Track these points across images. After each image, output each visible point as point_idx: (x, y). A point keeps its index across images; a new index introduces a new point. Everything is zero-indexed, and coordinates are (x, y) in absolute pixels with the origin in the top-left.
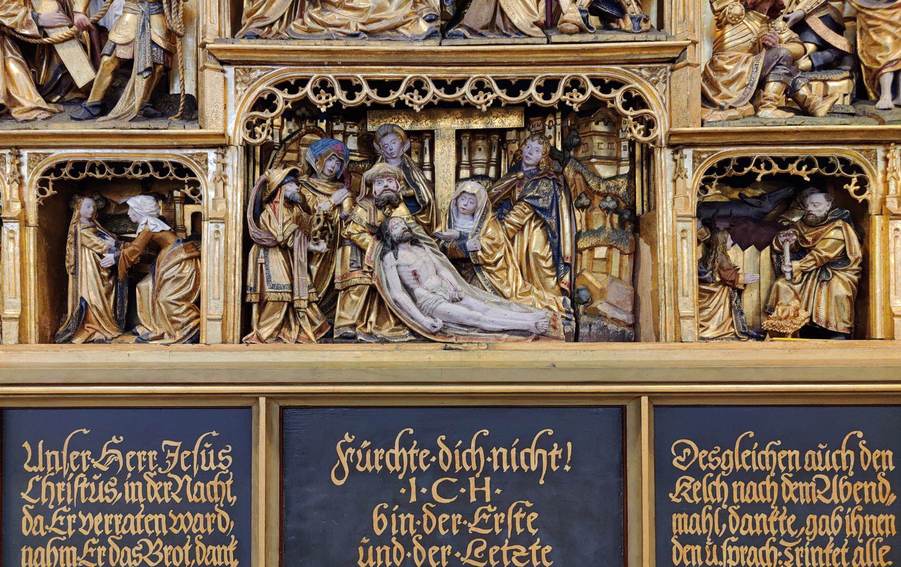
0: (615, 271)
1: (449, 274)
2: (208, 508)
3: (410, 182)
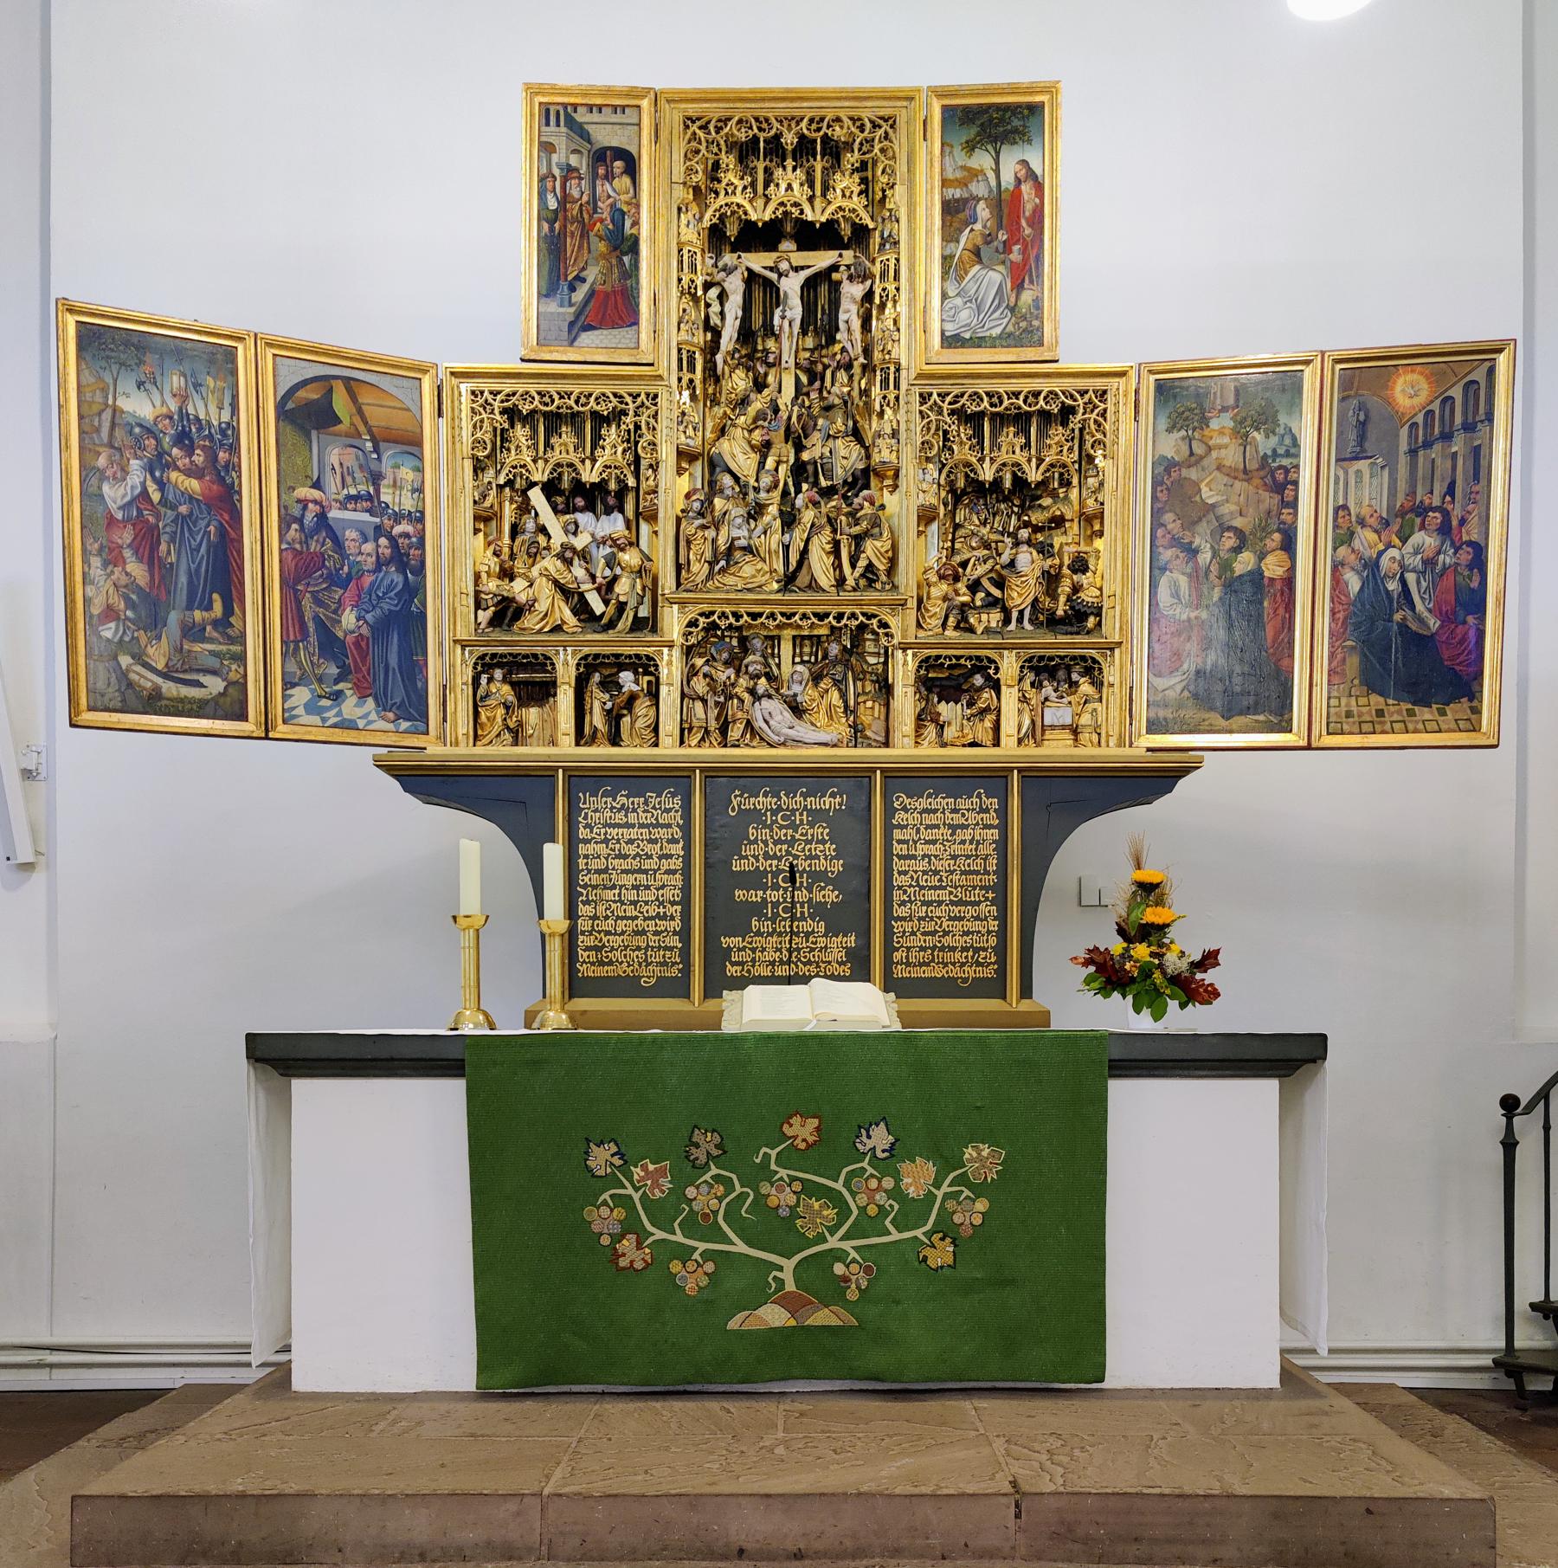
2: (669, 826)
3: (767, 665)
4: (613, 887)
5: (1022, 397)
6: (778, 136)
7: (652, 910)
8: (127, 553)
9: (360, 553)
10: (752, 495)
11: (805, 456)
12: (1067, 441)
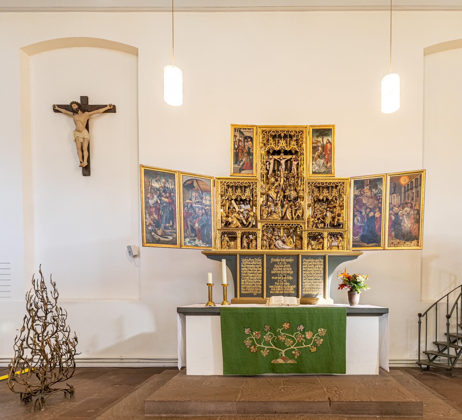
1: (282, 243)
2: (259, 265)
3: (278, 234)
4: (248, 276)
6: (280, 134)
7: (256, 281)
8: (154, 213)
10: (275, 202)
11: (286, 194)
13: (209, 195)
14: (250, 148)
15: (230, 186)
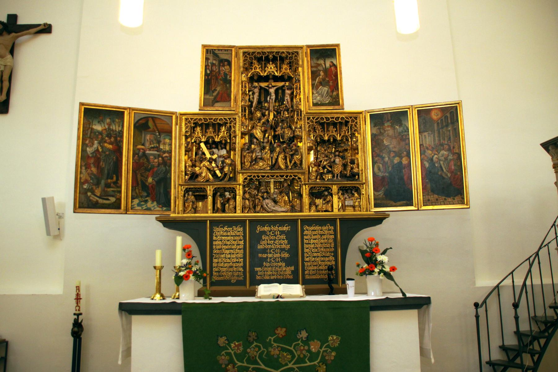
0: (298, 203)
1: (273, 203)
2: (239, 236)
3: (266, 189)
4: (223, 254)
5: (335, 118)
6: (268, 56)
7: (235, 260)
8: (92, 165)
9: (154, 162)
10: (262, 144)
11: (277, 133)
12: (347, 130)
13: (169, 137)
14: (228, 73)
15: (198, 123)
